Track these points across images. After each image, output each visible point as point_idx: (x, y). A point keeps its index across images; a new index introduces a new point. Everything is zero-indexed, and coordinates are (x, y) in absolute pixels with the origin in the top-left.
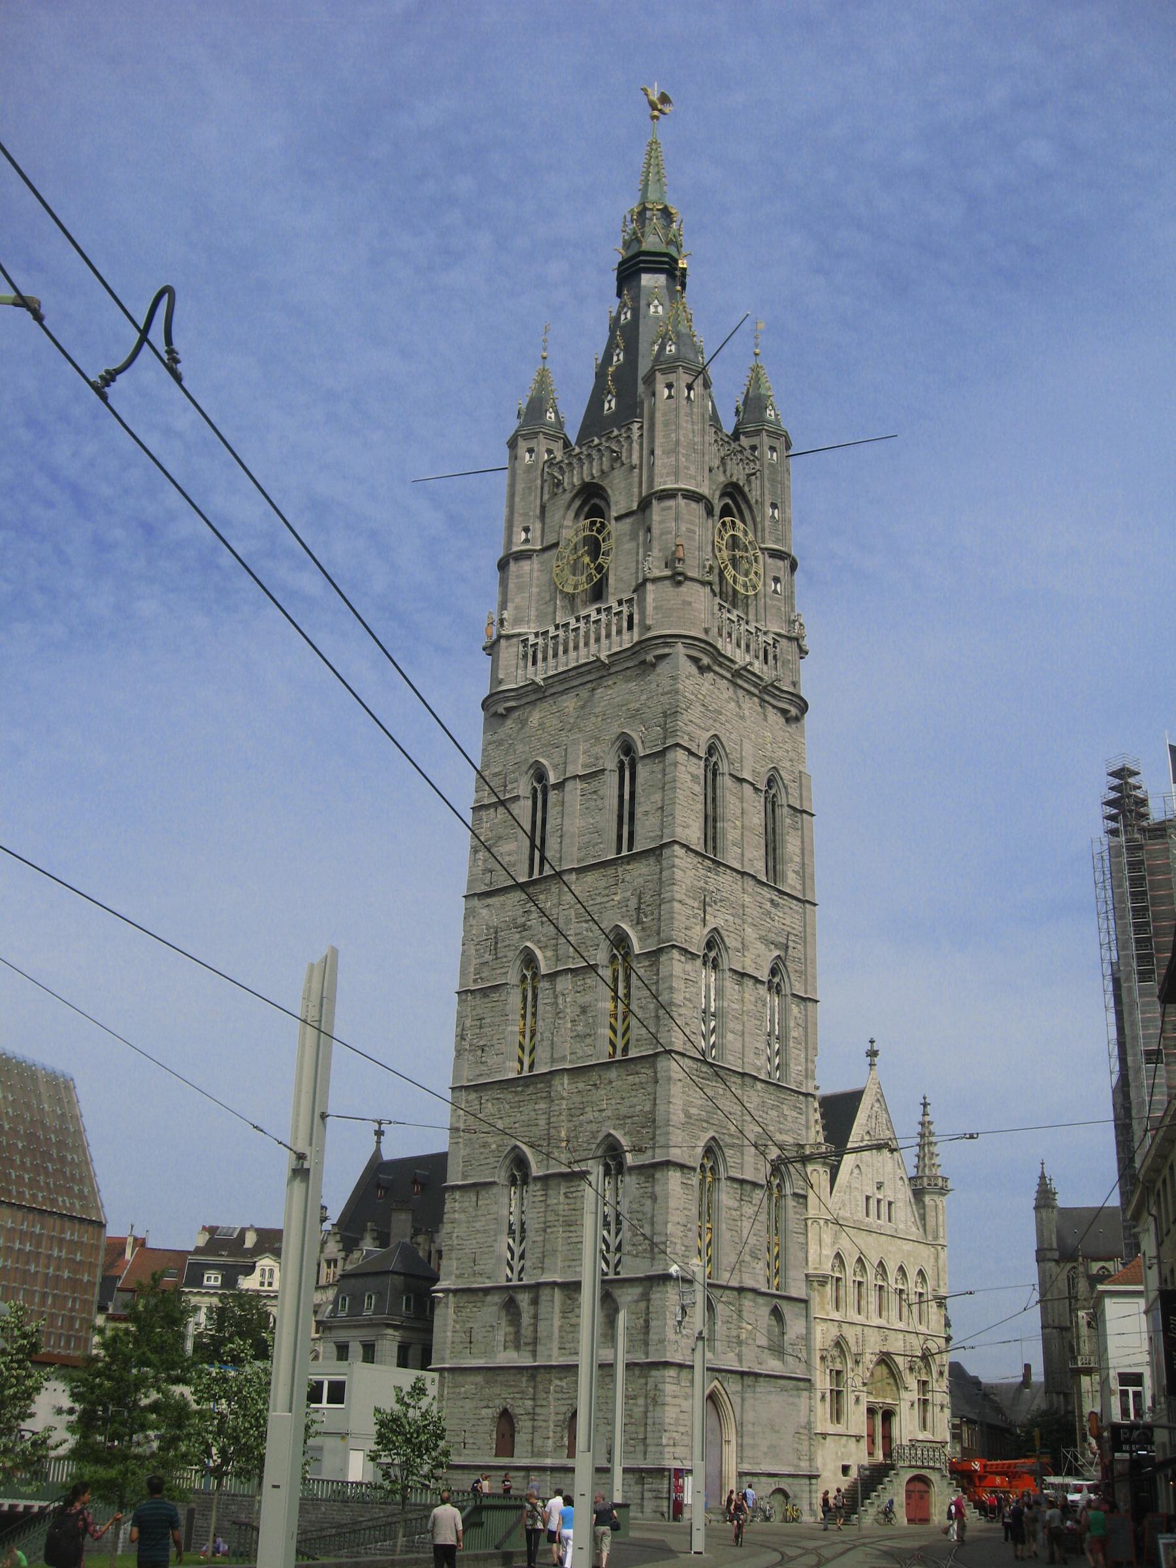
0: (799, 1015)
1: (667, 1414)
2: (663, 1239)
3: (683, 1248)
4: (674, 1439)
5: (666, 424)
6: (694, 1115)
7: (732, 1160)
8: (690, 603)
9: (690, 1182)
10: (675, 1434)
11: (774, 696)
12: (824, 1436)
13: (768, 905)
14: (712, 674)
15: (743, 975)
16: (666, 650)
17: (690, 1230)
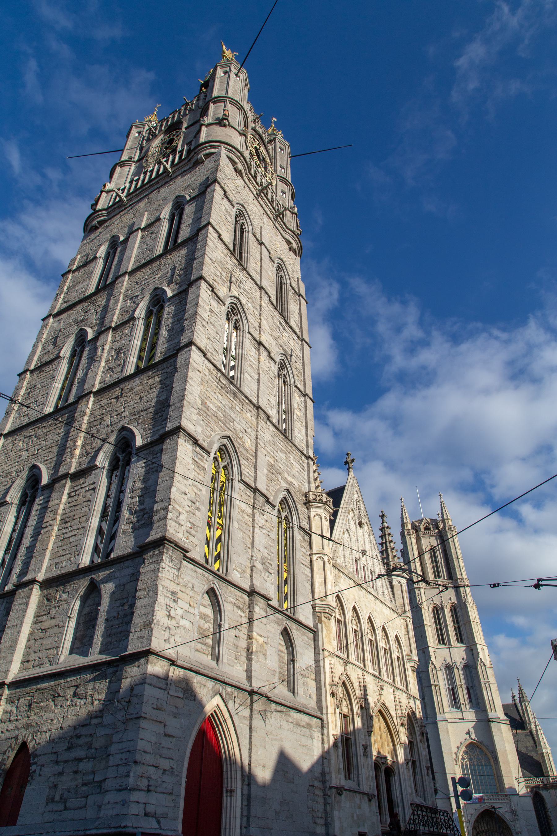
0: (300, 403)
1: (142, 734)
2: (164, 505)
3: (189, 525)
4: (149, 778)
5: (221, 82)
6: (211, 409)
7: (246, 469)
8: (231, 137)
9: (202, 464)
10: (152, 769)
11: (283, 229)
12: (340, 790)
13: (278, 323)
14: (242, 181)
15: (260, 343)
16: (213, 150)
17: (198, 509)
